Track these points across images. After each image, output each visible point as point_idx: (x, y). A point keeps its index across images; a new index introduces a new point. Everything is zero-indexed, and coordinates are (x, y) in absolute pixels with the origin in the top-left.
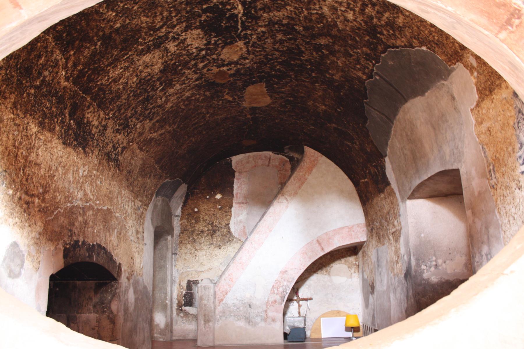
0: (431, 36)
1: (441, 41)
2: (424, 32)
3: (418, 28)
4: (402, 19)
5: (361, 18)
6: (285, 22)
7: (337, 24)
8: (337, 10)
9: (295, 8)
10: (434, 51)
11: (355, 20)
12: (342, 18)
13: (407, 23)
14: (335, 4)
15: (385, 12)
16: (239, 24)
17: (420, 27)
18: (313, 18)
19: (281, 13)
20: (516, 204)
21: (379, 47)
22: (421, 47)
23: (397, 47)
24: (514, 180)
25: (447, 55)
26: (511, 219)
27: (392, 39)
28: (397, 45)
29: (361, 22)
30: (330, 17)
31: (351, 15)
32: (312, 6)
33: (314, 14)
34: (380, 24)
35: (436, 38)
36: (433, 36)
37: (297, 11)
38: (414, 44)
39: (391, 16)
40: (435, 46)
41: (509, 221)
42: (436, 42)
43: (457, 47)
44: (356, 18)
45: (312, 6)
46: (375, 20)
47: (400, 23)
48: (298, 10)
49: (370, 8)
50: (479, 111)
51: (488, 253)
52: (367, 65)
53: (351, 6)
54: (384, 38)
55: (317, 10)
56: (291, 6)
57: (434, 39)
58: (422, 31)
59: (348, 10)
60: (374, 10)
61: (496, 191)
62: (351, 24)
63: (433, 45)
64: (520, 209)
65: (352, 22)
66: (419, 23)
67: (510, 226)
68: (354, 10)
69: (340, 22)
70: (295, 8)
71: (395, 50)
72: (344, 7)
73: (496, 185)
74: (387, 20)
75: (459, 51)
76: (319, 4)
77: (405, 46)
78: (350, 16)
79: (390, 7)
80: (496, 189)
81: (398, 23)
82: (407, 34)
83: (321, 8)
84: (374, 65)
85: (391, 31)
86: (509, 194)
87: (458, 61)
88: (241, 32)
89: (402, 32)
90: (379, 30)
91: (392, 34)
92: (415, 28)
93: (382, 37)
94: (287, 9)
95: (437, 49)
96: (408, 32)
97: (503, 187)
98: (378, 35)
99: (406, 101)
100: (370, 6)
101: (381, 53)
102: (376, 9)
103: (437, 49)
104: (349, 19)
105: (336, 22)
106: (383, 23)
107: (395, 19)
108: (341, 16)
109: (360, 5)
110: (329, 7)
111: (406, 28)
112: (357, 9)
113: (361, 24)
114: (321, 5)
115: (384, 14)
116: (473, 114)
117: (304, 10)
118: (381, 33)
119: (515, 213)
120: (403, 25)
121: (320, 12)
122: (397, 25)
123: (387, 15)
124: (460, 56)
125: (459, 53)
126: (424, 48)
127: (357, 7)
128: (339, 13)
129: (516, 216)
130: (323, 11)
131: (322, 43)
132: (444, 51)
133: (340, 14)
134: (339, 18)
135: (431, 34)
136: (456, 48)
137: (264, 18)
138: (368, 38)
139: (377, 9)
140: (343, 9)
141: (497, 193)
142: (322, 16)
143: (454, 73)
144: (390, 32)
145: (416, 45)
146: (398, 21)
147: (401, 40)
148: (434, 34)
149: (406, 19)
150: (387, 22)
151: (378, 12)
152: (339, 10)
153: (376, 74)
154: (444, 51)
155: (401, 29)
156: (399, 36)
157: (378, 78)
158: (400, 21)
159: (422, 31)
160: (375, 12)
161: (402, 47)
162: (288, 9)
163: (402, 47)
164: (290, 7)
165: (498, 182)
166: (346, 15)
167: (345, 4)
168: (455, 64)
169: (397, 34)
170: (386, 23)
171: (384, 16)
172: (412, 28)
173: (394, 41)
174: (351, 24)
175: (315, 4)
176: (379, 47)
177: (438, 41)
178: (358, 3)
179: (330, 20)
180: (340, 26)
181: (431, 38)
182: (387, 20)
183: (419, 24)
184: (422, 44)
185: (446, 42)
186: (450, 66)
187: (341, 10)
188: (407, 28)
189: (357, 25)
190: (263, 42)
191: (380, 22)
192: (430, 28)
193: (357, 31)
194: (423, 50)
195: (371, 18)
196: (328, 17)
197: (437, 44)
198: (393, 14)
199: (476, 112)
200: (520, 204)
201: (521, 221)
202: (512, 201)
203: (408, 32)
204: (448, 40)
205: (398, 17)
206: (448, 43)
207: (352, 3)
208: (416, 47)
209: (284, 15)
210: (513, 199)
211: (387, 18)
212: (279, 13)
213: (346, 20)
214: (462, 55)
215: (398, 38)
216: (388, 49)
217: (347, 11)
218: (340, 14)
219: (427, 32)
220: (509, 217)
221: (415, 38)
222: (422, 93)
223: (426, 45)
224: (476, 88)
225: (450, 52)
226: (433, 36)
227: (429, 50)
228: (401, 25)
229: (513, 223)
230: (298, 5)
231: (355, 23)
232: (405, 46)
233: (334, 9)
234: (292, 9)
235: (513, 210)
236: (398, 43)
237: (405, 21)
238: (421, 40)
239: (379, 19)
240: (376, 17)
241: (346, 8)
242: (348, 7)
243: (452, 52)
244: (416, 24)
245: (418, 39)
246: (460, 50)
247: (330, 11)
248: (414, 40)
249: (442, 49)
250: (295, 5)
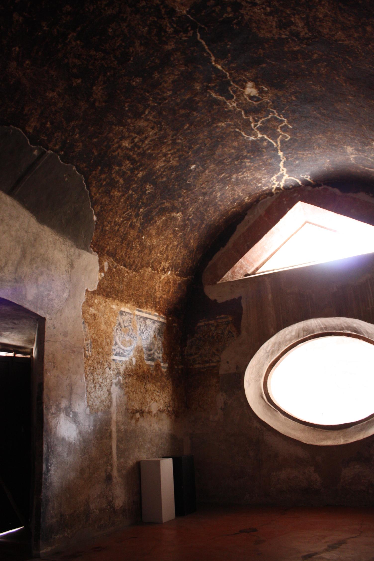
0: (107, 223)
1: (106, 233)
2: (109, 216)
3: (111, 210)
4: (117, 196)
5: (121, 155)
6: (156, 75)
7: (121, 126)
8: (137, 134)
9: (165, 99)
10: (96, 229)
11: (120, 147)
12: (127, 134)
13: (114, 200)
14: (144, 135)
15: (124, 180)
16: (206, 47)
17: (112, 212)
18: (140, 106)
19: (170, 81)
20: (104, 377)
21: (84, 165)
22: (95, 214)
23: (88, 188)
24: (107, 361)
25: (97, 241)
26: (98, 386)
27: (96, 183)
28: (91, 188)
29: (116, 153)
30: (132, 123)
31: (127, 145)
32: (154, 114)
33: (145, 110)
34: (113, 172)
35: (107, 228)
36: (107, 225)
37: (159, 97)
38: (96, 207)
39: (120, 185)
40: (101, 229)
41: (95, 386)
42: (104, 229)
43: (107, 249)
44: (122, 149)
45: (154, 114)
46: (117, 168)
47: (114, 193)
48: (160, 99)
49: (130, 166)
50: (92, 297)
51: (68, 407)
52: (54, 140)
53: (136, 149)
54: (96, 174)
55: (147, 115)
56: (169, 97)
57: (106, 227)
58: (109, 214)
59: (133, 144)
60: (127, 170)
61: (87, 361)
62: (116, 140)
63: (101, 227)
64: (106, 381)
65: (118, 142)
66: (115, 211)
67: (95, 390)
68: (131, 150)
69: (122, 131)
70: (165, 99)
71: (84, 185)
72: (138, 142)
73: (90, 357)
74: (116, 180)
75: (105, 251)
76: (152, 121)
77: (92, 198)
78: (126, 144)
79: (128, 185)
80: (89, 360)
81: (113, 191)
82: (104, 199)
83: (147, 120)
84: (57, 152)
85: (105, 183)
86: (99, 368)
87: (98, 253)
88: (195, 34)
89: (105, 194)
90: (106, 170)
91: (102, 184)
92: (110, 207)
93: (98, 172)
94: (169, 90)
95: (99, 231)
96: (106, 200)
97: (95, 361)
98: (100, 168)
99: (10, 193)
100: (131, 166)
101: (76, 167)
102: (127, 171)
103: (99, 231)
104: (123, 142)
105: (124, 126)
106: (114, 175)
107: (117, 189)
108: (129, 134)
109: (135, 158)
110: (144, 128)
111: (109, 198)
112: (131, 153)
113: (114, 151)
114: (149, 122)
115: (122, 178)
116: (86, 294)
117: (156, 104)
118: (102, 172)
119: (102, 383)
120: (112, 196)
121: (143, 116)
122: (112, 189)
123: (121, 181)
124: (102, 254)
125: (104, 251)
126: (95, 218)
127: (133, 154)
128: (134, 135)
129: (102, 385)
130: (143, 120)
131: (94, 88)
132: (99, 238)
133: (131, 134)
134: (127, 131)
135: (108, 223)
136: (106, 248)
137: (181, 62)
138: (96, 154)
139: (127, 173)
140: (136, 140)
141: (88, 362)
142: (138, 115)
143: (88, 254)
144: (104, 181)
145: (95, 209)
146: (115, 191)
147: (97, 193)
148: (109, 225)
149: (117, 198)
150: (114, 180)
151: (124, 173)
152: (136, 135)
153: (42, 154)
154: (99, 238)
155: (107, 193)
156: (100, 191)
157: (36, 152)
158: (116, 193)
159: (109, 214)
160: (125, 170)
161: (90, 194)
162: (168, 92)
163: (90, 194)
164: (169, 95)
165: (92, 355)
166: (129, 140)
167: (140, 145)
168: (95, 251)
169: (102, 189)
170: (113, 179)
171: (120, 178)
172: (110, 205)
173: (94, 185)
174: (116, 140)
175: (154, 117)
176: (84, 165)
177: (106, 230)
178: (137, 157)
179: (129, 121)
180: (118, 128)
181: (106, 223)
182: (116, 180)
183: (114, 210)
184: (97, 215)
185: (107, 238)
186: (91, 247)
187: (135, 137)
188: (109, 199)
189: (114, 147)
190: (148, 22)
191: (115, 172)
192: (113, 221)
193: (105, 144)
194: (93, 217)
195: (120, 165)
196: (133, 121)
197: (102, 230)
198: (122, 187)
199: (90, 296)
200: (108, 378)
201: (107, 389)
202: (102, 374)
203: (105, 200)
204: (109, 239)
205: (119, 191)
206: (107, 240)
207: (139, 151)
208: (94, 209)
209: (166, 82)
210: (103, 373)
211: (118, 181)
212: (172, 80)
213: (123, 138)
214: (104, 255)
215: (99, 190)
216: (83, 176)
217: (132, 143)
218: (131, 134)
219: (109, 219)
220: (96, 383)
221: (101, 207)
222: (41, 220)
223: (98, 220)
224: (99, 283)
225: (101, 244)
226: (107, 225)
227: (95, 223)
228: (112, 194)
229: (99, 389)
230: (165, 104)
231: (117, 145)
232: (92, 198)
233: (140, 132)
234: (165, 95)
235: (101, 380)
236: (94, 190)
237: (116, 198)
238: (101, 213)
239: (118, 173)
240: (120, 170)
241: (136, 143)
242: (136, 145)
243: (102, 245)
244: (114, 207)
245: (101, 211)
246: (106, 252)
247: (140, 126)
248: (99, 207)
249: (100, 236)
250: (167, 101)
